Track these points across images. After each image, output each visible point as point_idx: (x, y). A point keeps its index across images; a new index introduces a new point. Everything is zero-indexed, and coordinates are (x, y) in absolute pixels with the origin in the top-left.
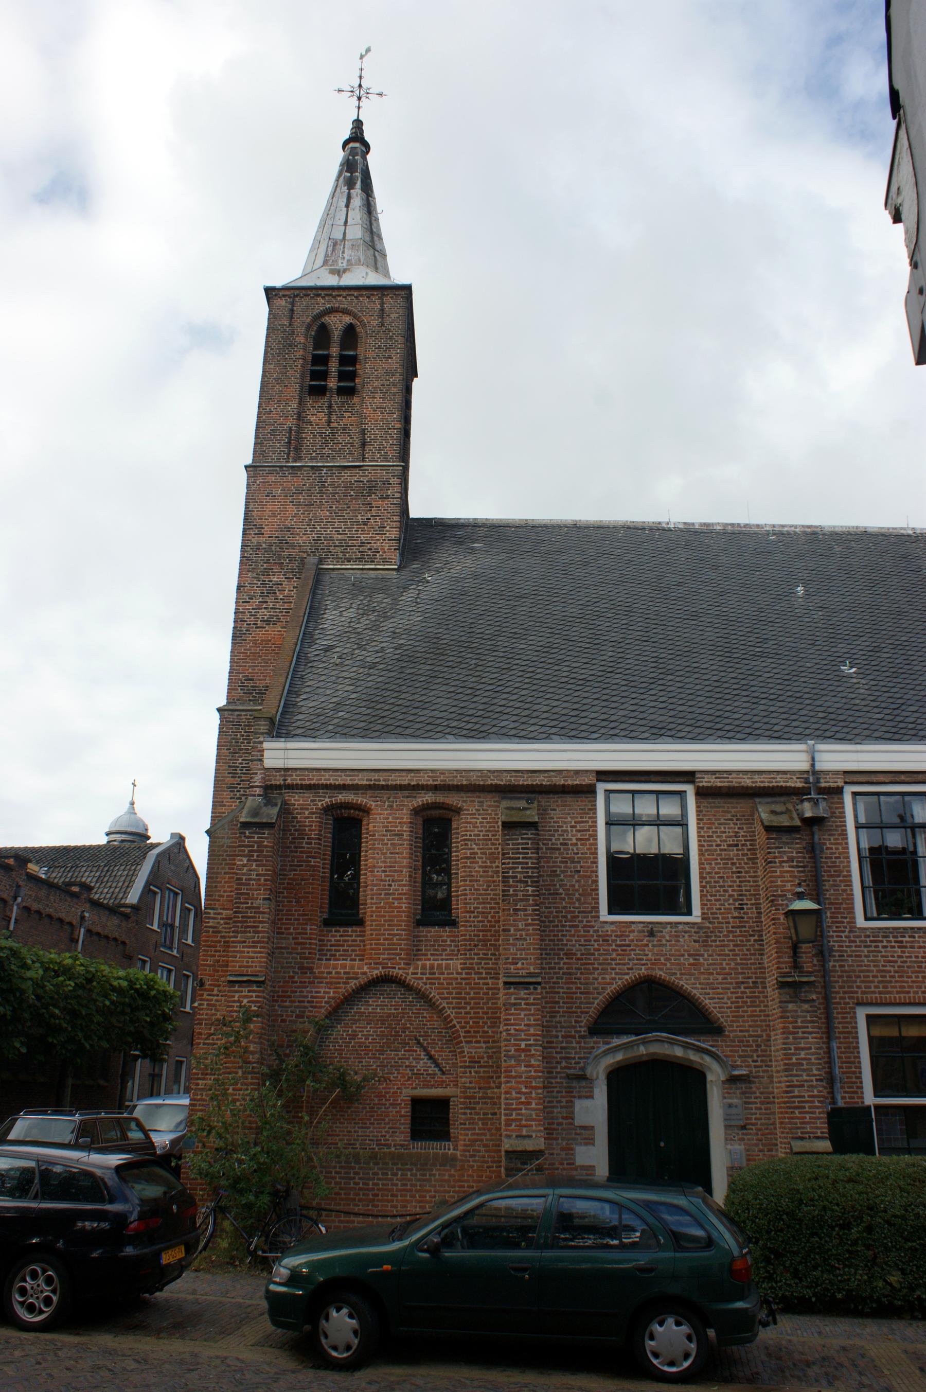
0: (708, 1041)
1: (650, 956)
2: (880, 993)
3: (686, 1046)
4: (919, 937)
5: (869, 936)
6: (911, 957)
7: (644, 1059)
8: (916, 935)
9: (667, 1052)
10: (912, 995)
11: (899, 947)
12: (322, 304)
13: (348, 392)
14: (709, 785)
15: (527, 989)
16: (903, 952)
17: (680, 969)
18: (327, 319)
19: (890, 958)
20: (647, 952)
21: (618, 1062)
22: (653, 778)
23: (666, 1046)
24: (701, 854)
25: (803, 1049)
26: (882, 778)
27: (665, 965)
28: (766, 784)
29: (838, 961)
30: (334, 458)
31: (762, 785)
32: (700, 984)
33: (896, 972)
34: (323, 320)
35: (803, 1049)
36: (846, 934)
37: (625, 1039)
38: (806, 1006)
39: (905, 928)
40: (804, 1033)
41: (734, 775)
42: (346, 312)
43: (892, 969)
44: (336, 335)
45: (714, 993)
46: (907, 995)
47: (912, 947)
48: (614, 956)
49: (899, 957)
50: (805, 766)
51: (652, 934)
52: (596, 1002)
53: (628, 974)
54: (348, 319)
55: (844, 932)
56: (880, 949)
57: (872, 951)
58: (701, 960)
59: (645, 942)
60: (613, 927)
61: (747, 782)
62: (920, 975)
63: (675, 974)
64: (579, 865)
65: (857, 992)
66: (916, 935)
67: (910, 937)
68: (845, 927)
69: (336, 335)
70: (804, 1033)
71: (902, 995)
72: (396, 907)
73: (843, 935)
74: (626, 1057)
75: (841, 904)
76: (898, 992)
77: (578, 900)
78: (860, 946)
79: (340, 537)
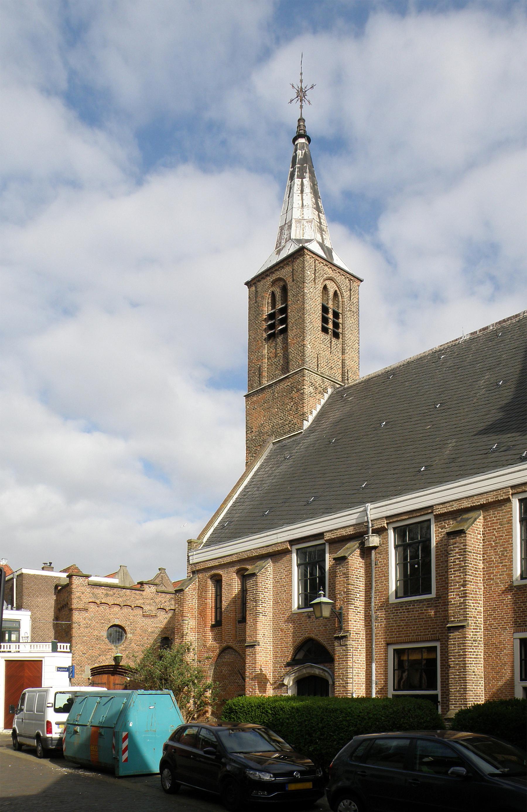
4: (417, 605)
5: (394, 608)
6: (412, 617)
8: (416, 604)
10: (411, 637)
11: (407, 612)
16: (409, 614)
17: (319, 633)
19: (403, 619)
20: (308, 626)
24: (330, 575)
27: (314, 631)
29: (380, 622)
32: (327, 639)
33: (405, 626)
40: (342, 661)
43: (403, 624)
47: (413, 611)
49: (407, 617)
53: (301, 637)
56: (399, 614)
57: (395, 616)
59: (307, 621)
60: (296, 616)
62: (416, 626)
63: (318, 635)
64: (285, 588)
67: (413, 606)
70: (342, 661)
72: (229, 617)
76: (405, 637)
77: (285, 605)
78: (389, 614)
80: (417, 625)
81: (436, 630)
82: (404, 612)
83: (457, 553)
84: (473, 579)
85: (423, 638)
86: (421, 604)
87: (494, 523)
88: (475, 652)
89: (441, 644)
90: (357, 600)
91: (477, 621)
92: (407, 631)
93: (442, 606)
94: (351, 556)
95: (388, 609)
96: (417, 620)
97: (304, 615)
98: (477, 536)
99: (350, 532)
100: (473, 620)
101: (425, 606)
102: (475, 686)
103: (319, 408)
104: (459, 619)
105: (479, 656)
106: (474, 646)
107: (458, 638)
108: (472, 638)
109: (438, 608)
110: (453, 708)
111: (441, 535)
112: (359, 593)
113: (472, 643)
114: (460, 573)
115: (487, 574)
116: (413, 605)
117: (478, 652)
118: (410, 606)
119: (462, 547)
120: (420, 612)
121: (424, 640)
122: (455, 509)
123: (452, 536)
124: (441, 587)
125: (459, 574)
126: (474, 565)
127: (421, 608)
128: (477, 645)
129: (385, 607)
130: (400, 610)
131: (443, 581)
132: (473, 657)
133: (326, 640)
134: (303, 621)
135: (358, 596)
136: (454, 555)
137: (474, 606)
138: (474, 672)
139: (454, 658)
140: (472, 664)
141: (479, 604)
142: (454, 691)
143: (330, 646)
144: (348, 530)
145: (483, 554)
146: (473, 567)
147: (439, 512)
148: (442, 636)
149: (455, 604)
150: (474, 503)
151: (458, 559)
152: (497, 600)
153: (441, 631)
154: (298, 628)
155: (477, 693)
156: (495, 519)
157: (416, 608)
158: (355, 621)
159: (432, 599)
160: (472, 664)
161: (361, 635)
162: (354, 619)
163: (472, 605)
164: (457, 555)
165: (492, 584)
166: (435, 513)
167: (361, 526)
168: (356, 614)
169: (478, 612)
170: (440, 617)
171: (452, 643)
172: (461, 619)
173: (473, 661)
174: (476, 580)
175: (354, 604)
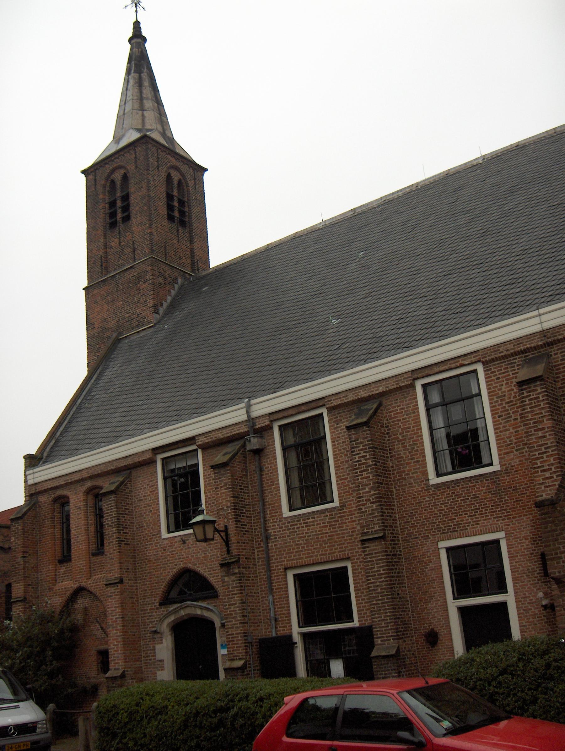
0: (213, 603)
1: (184, 556)
2: (297, 559)
3: (201, 608)
4: (318, 517)
5: (290, 522)
6: (312, 532)
7: (186, 618)
8: (316, 516)
9: (193, 613)
10: (314, 558)
11: (306, 526)
12: (109, 168)
13: (126, 219)
14: (202, 443)
15: (114, 587)
16: (308, 529)
18: (113, 177)
19: (301, 535)
21: (173, 621)
22: (179, 445)
23: (193, 609)
25: (232, 605)
26: (291, 412)
28: (229, 435)
30: (124, 265)
31: (227, 435)
33: (305, 544)
34: (112, 178)
35: (232, 605)
36: (278, 523)
37: (176, 606)
38: (233, 578)
39: (309, 513)
41: (213, 433)
42: (120, 167)
44: (118, 183)
45: (215, 573)
46: (311, 559)
48: (168, 559)
50: (245, 417)
51: (184, 542)
52: (162, 587)
54: (122, 171)
55: (276, 522)
56: (296, 530)
58: (208, 554)
61: (220, 435)
63: (196, 564)
65: (284, 561)
66: (316, 516)
67: (312, 518)
68: (277, 519)
69: (118, 183)
71: (341, 553)
73: (276, 524)
74: (176, 617)
75: (275, 503)
78: (285, 530)
79: (128, 315)
80: (320, 541)
81: (344, 546)
82: (302, 527)
83: (361, 450)
84: (383, 480)
85: (329, 557)
86: (322, 515)
87: (397, 413)
88: (396, 569)
89: (352, 564)
90: (243, 516)
91: (394, 530)
92: (309, 550)
93: (348, 516)
94: (232, 462)
95: (283, 524)
96: (320, 536)
97: (176, 539)
98: (380, 429)
99: (227, 434)
100: (390, 530)
101: (327, 518)
102: (402, 611)
103: (169, 299)
104: (373, 530)
105: (401, 574)
106: (395, 562)
107: (375, 553)
108: (391, 552)
109: (344, 518)
110: (379, 642)
111: (338, 431)
112: (245, 507)
113: (392, 559)
114: (367, 474)
115: (397, 473)
116: (314, 518)
117: (399, 569)
118: (309, 519)
119: (367, 443)
120: (322, 525)
121: (331, 559)
122: (351, 399)
123: (353, 430)
124: (344, 493)
125: (366, 475)
126: (382, 463)
127: (322, 520)
128: (397, 560)
129: (278, 523)
130: (297, 524)
131: (345, 486)
132: (395, 575)
133: (207, 570)
134: (176, 548)
135: (244, 511)
136: (358, 452)
137: (388, 513)
138: (398, 594)
139: (373, 579)
140: (394, 584)
141: (393, 509)
142: (379, 621)
143: (213, 577)
144: (224, 431)
145: (390, 450)
146: (381, 466)
147: (333, 405)
148: (353, 553)
149: (366, 511)
150: (373, 391)
151: (363, 457)
152: (413, 504)
153: (350, 546)
154: (170, 557)
155: (405, 621)
156: (398, 408)
157: (317, 521)
158: (244, 543)
159: (335, 508)
160: (394, 584)
161: (252, 560)
162: (241, 540)
163: (386, 511)
164: (362, 452)
165: (406, 485)
166: (327, 406)
167: (240, 426)
168: (244, 534)
169: (393, 520)
170: (347, 529)
171: (369, 559)
172: (376, 529)
173: (396, 580)
174: (386, 481)
175: (241, 522)
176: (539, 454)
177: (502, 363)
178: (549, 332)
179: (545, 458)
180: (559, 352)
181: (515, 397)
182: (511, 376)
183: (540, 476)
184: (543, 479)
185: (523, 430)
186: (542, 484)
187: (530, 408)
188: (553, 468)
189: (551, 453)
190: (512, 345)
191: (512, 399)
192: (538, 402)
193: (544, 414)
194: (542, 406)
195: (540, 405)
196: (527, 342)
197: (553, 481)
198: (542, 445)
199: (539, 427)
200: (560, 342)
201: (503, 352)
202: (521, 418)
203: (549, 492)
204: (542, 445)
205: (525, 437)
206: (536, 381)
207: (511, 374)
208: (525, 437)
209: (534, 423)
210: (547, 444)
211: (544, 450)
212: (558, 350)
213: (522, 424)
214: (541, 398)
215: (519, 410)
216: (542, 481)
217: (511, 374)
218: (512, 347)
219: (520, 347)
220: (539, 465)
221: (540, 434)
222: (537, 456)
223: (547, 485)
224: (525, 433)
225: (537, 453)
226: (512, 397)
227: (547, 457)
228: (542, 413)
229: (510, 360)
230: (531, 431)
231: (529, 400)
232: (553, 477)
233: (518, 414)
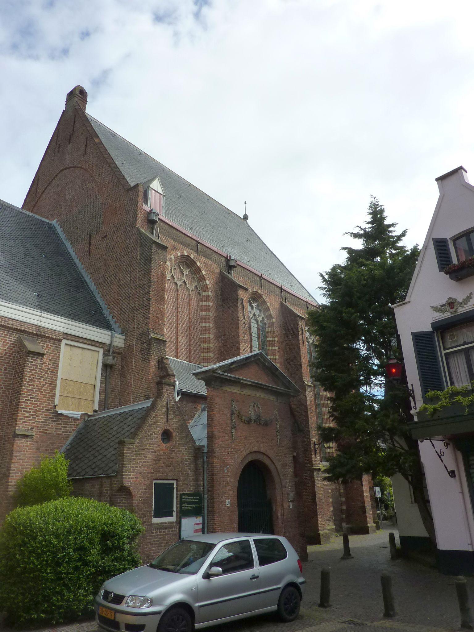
176: (26, 400)
177: (5, 330)
178: (42, 329)
179: (28, 404)
180: (42, 342)
181: (5, 355)
182: (8, 341)
183: (22, 414)
184: (23, 417)
185: (3, 378)
186: (22, 419)
187: (30, 370)
188: (32, 411)
189: (33, 402)
190: (17, 323)
191: (3, 356)
192: (36, 368)
193: (37, 377)
194: (37, 372)
195: (36, 371)
196: (27, 327)
197: (29, 420)
198: (29, 395)
199: (31, 383)
200: (48, 339)
201: (10, 324)
202: (5, 370)
203: (25, 426)
204: (29, 395)
205: (3, 383)
206: (39, 356)
207: (8, 340)
208: (3, 383)
209: (29, 379)
210: (33, 395)
211: (29, 399)
212: (42, 341)
213: (4, 374)
214: (38, 367)
215: (5, 364)
216: (22, 418)
217: (8, 340)
218: (17, 325)
219: (22, 327)
220: (24, 406)
221: (30, 388)
222: (24, 401)
223: (25, 421)
224: (4, 381)
225: (25, 399)
226: (3, 354)
227: (30, 403)
228: (36, 376)
229: (11, 332)
230: (26, 384)
231: (31, 364)
232: (30, 417)
233: (4, 367)
